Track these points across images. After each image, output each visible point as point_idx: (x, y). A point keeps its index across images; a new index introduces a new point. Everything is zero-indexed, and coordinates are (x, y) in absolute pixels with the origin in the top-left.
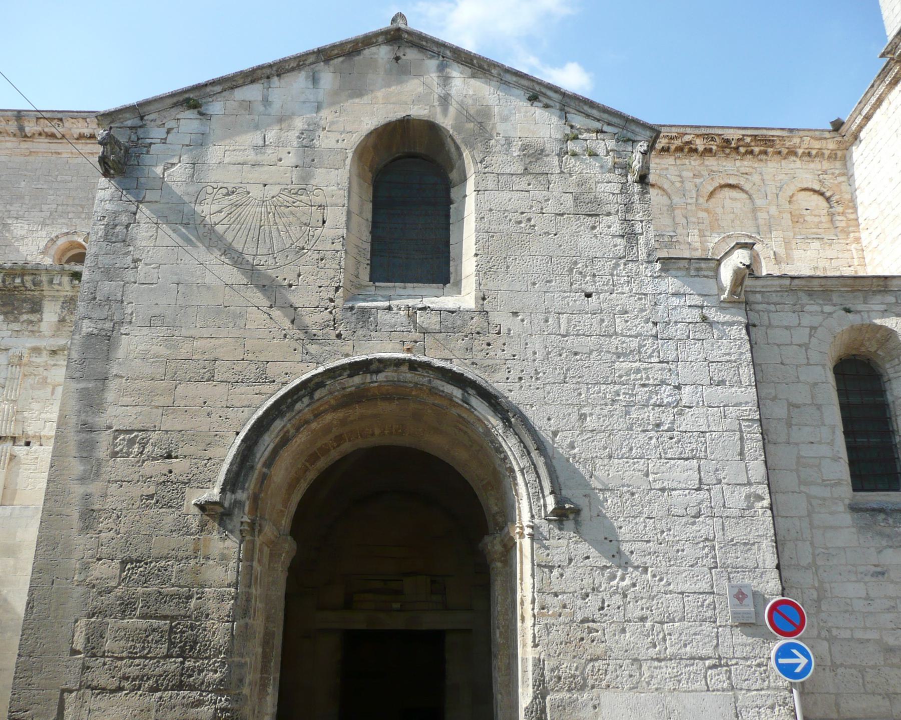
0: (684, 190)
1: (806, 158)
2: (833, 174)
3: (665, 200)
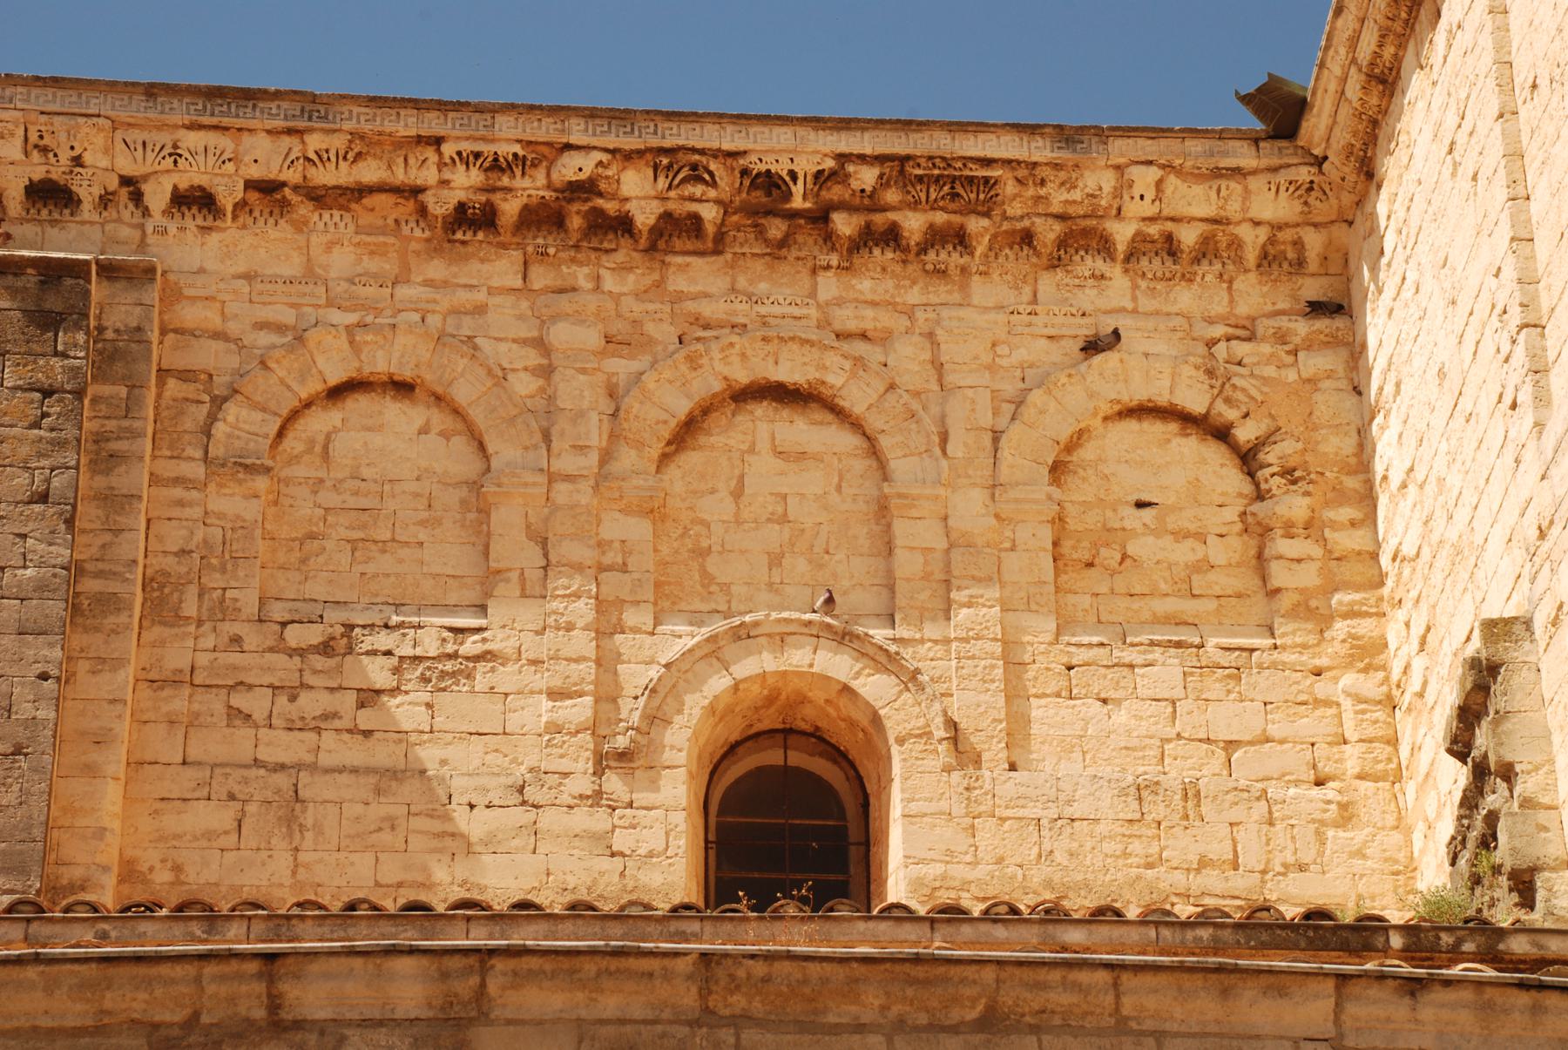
0: (551, 409)
1: (1153, 265)
2: (1281, 338)
3: (456, 459)
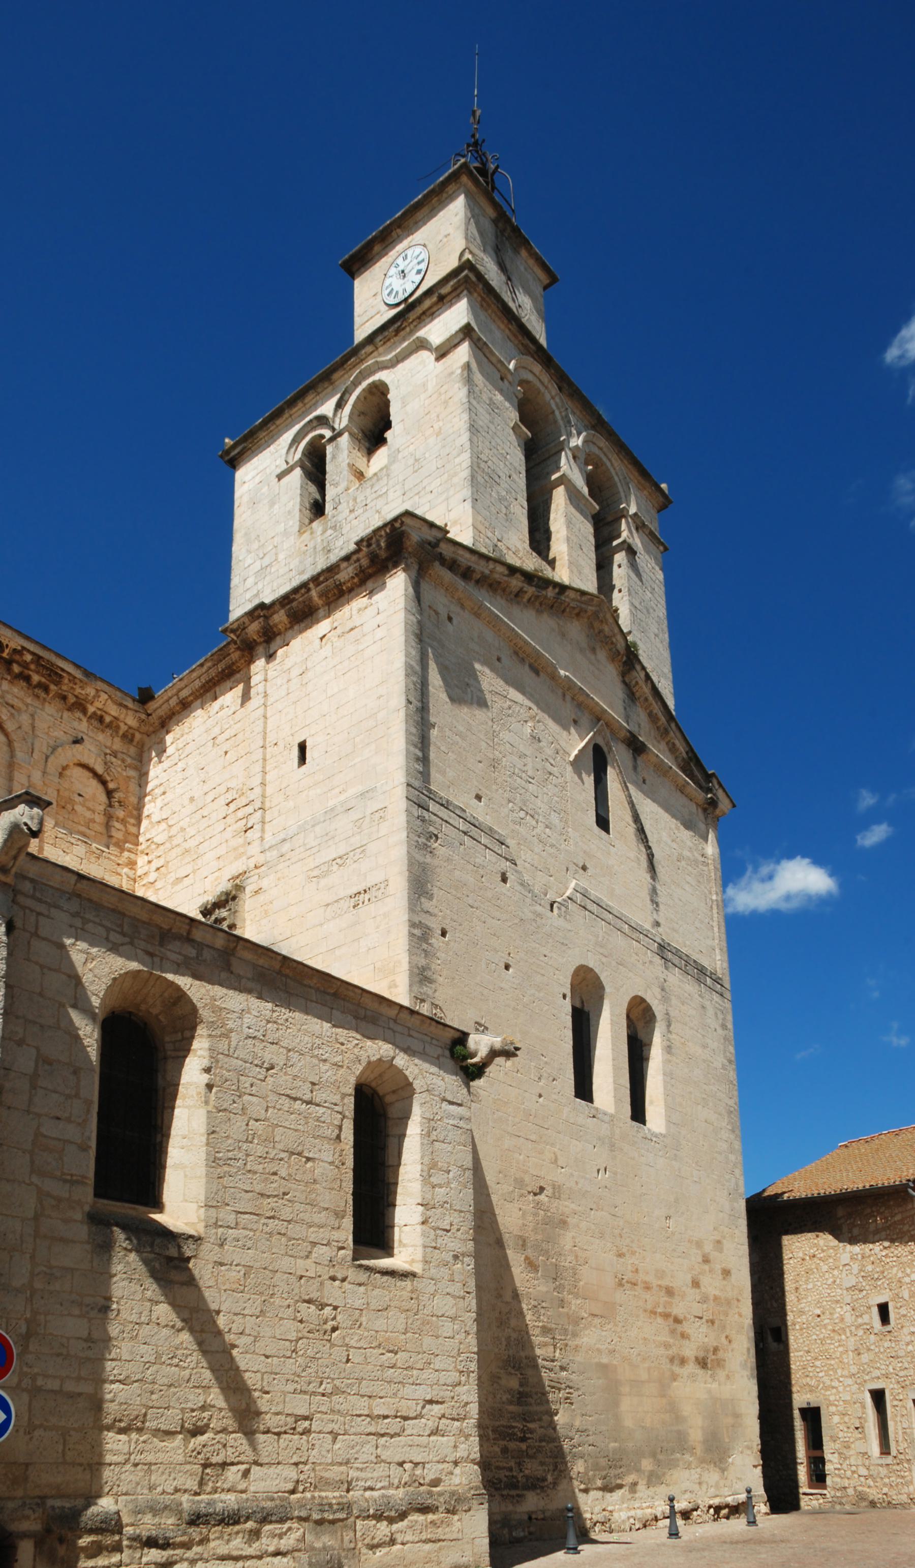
1: (95, 723)
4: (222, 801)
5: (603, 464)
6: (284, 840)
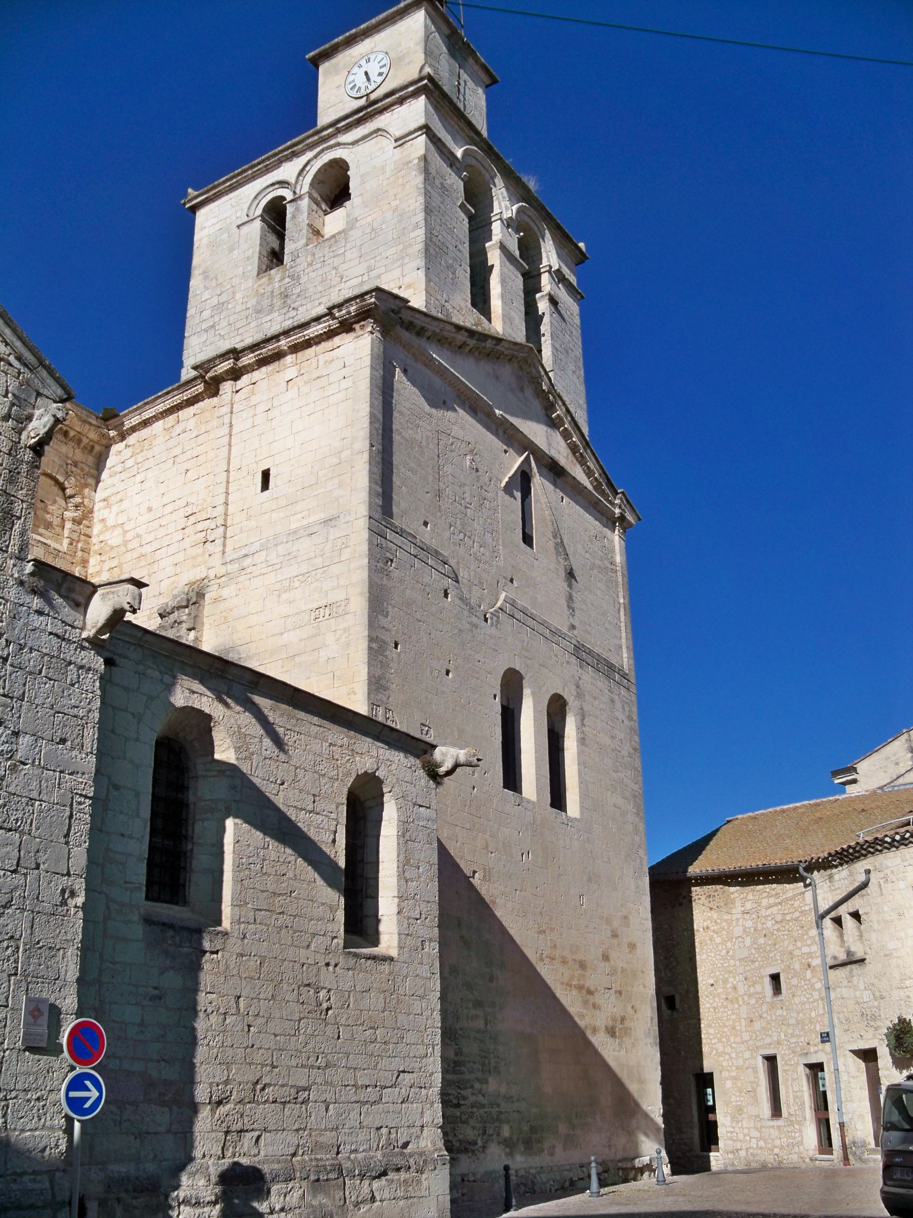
2: (82, 470)
4: (182, 513)
5: (531, 229)
6: (246, 556)
